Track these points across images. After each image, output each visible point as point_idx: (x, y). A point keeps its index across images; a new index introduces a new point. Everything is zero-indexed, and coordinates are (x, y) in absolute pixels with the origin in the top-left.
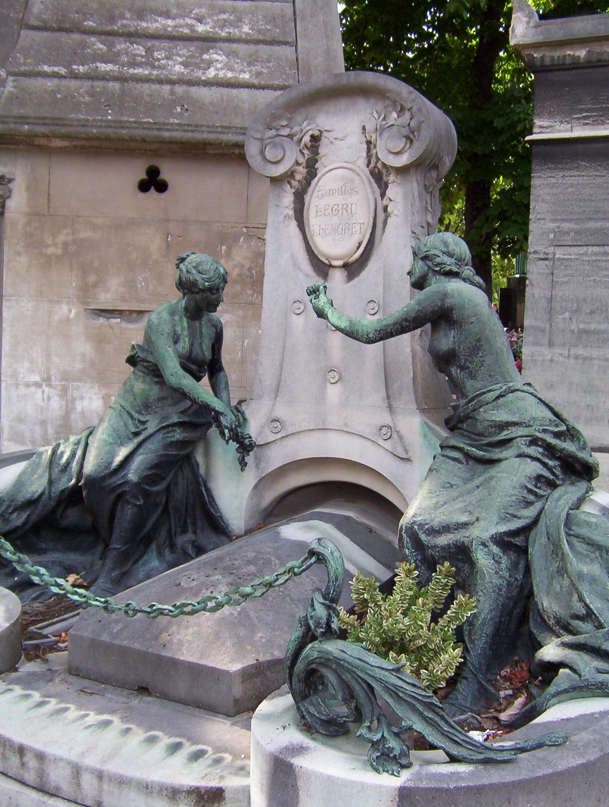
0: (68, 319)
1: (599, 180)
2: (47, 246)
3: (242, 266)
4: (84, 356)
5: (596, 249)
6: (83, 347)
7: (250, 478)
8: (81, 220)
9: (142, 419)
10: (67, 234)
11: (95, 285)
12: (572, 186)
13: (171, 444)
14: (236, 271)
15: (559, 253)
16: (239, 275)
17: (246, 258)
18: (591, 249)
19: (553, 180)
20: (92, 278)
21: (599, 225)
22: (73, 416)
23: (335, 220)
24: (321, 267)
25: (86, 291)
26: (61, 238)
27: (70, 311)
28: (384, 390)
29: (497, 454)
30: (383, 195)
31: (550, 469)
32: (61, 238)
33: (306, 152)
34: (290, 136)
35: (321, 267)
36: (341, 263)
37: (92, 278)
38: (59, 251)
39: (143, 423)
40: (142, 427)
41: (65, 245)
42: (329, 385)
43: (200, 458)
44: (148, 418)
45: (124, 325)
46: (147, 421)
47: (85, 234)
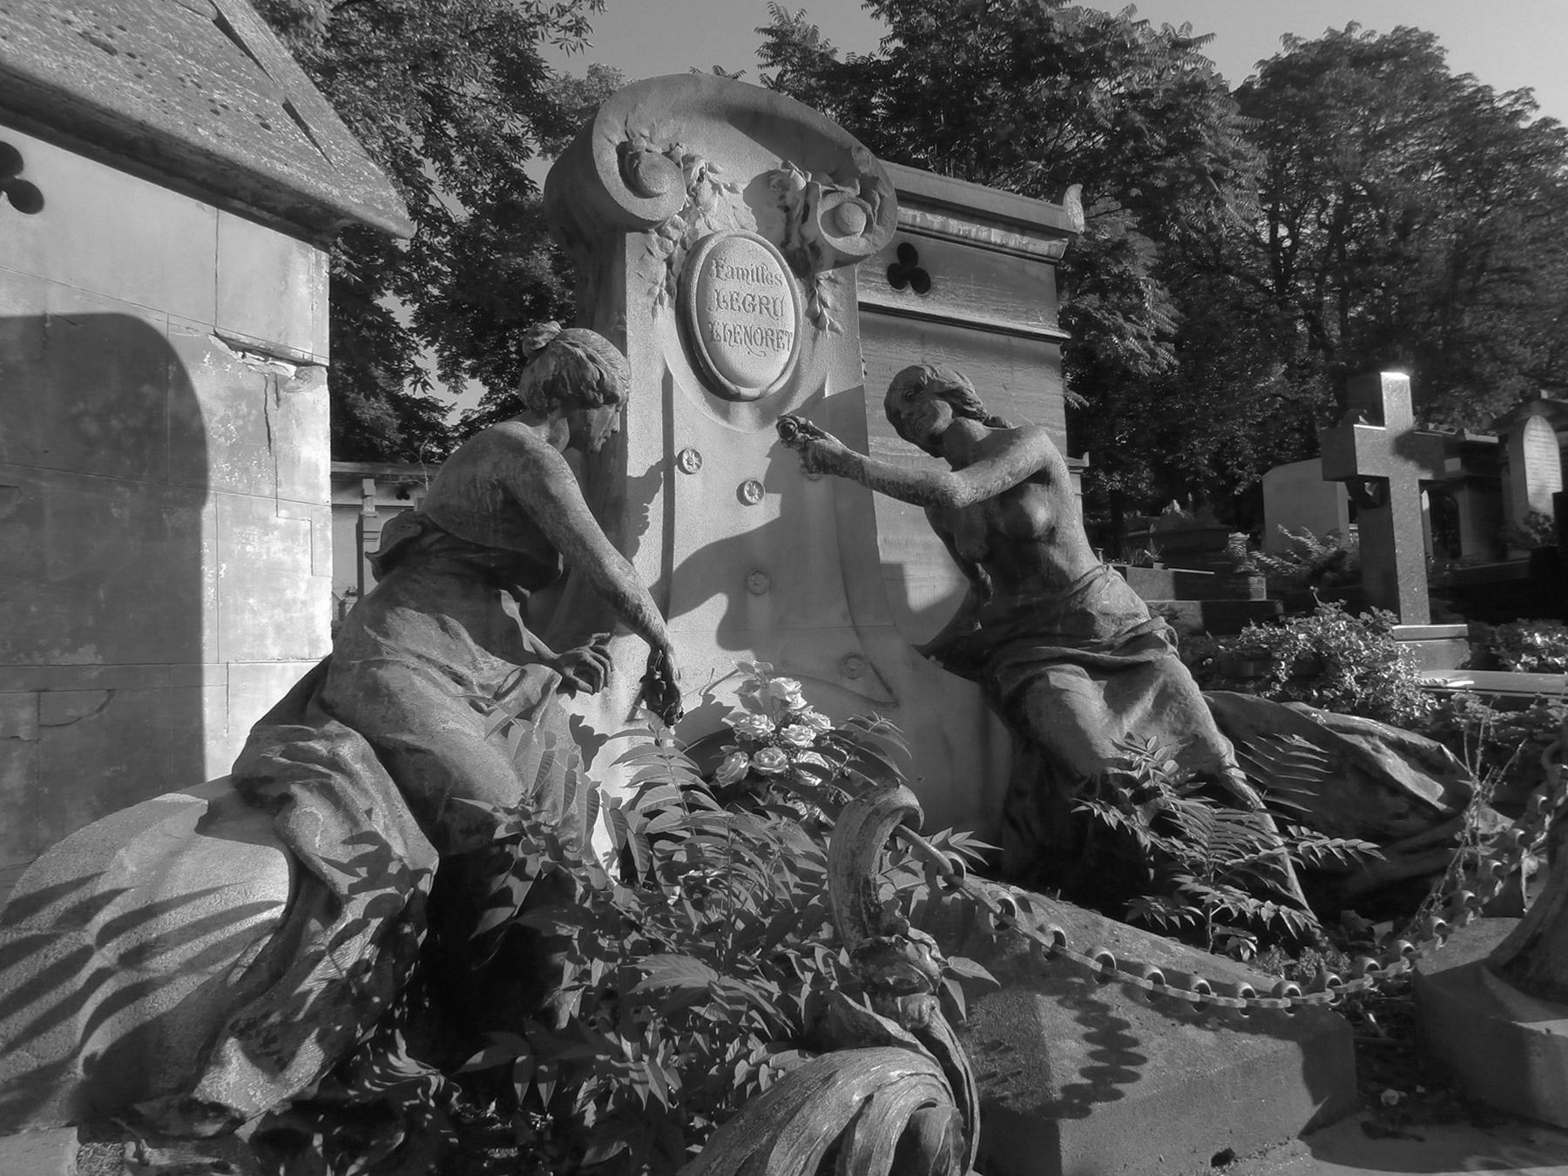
17: (218, 397)
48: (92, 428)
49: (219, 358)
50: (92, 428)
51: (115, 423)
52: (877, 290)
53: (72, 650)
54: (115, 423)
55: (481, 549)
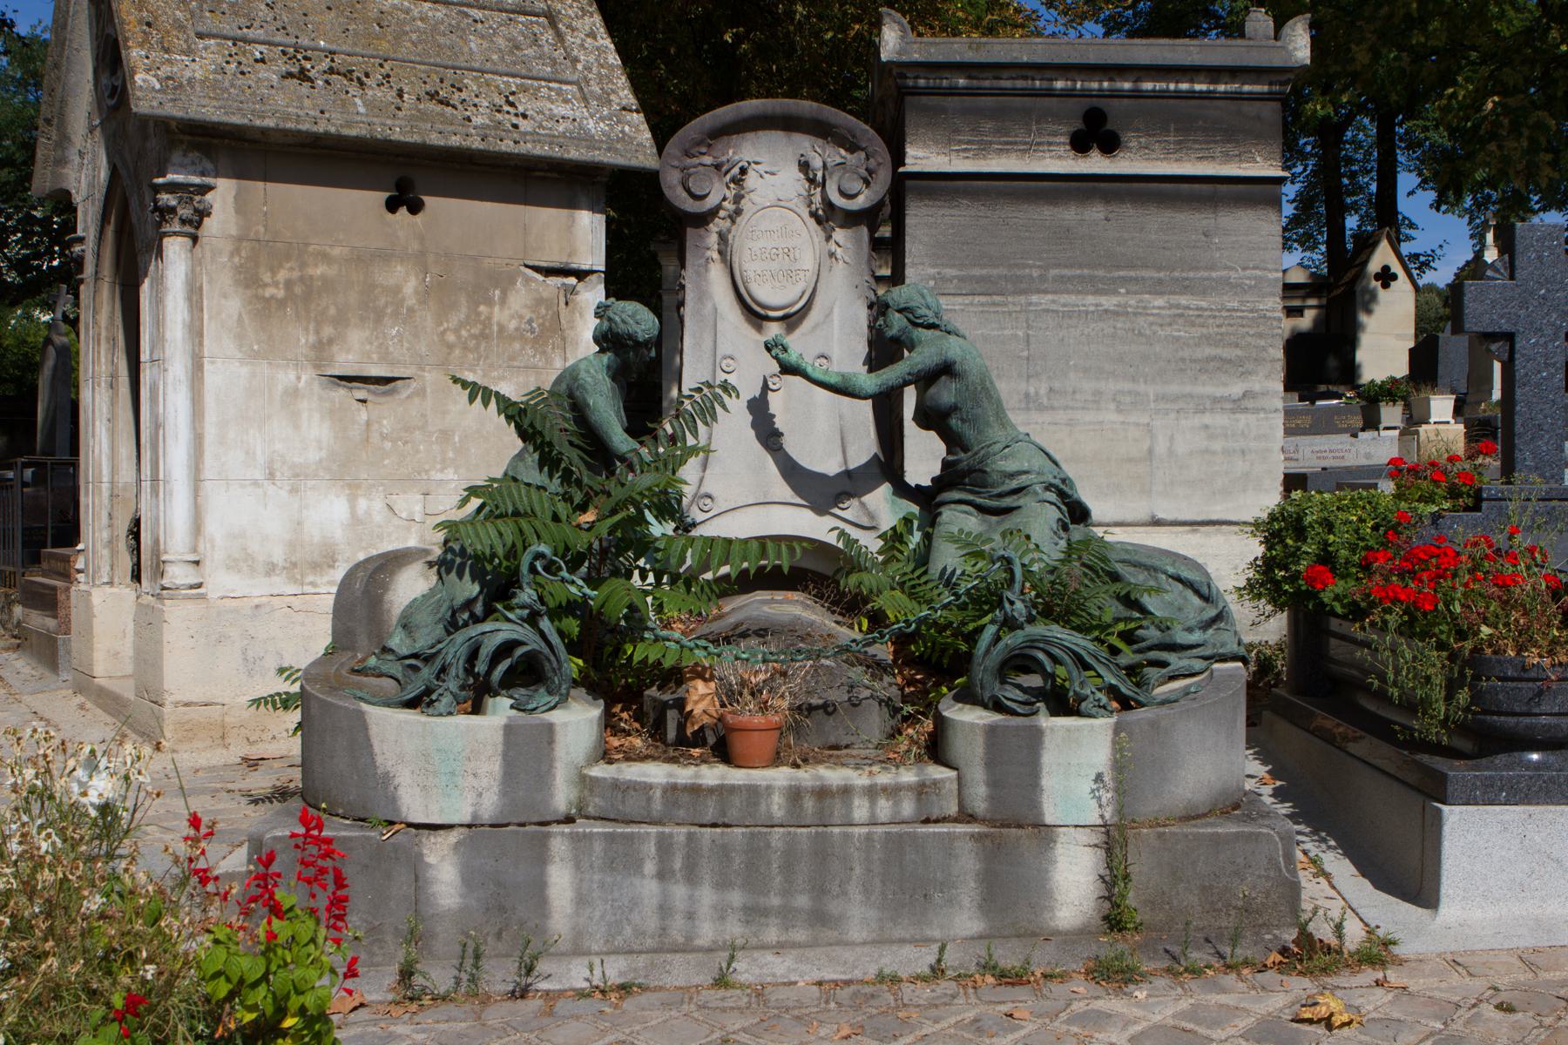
0: (296, 390)
2: (266, 285)
3: (521, 317)
4: (319, 441)
5: (983, 299)
8: (311, 249)
10: (292, 269)
11: (331, 341)
12: (953, 226)
14: (513, 325)
16: (517, 329)
17: (526, 306)
18: (977, 299)
19: (932, 220)
21: (984, 272)
23: (774, 266)
25: (321, 350)
26: (282, 275)
27: (299, 378)
29: (1008, 502)
30: (828, 238)
34: (718, 167)
35: (755, 315)
37: (328, 331)
38: (281, 294)
41: (289, 284)
47: (319, 270)
48: (451, 338)
49: (528, 280)
50: (451, 338)
51: (464, 333)
53: (442, 470)
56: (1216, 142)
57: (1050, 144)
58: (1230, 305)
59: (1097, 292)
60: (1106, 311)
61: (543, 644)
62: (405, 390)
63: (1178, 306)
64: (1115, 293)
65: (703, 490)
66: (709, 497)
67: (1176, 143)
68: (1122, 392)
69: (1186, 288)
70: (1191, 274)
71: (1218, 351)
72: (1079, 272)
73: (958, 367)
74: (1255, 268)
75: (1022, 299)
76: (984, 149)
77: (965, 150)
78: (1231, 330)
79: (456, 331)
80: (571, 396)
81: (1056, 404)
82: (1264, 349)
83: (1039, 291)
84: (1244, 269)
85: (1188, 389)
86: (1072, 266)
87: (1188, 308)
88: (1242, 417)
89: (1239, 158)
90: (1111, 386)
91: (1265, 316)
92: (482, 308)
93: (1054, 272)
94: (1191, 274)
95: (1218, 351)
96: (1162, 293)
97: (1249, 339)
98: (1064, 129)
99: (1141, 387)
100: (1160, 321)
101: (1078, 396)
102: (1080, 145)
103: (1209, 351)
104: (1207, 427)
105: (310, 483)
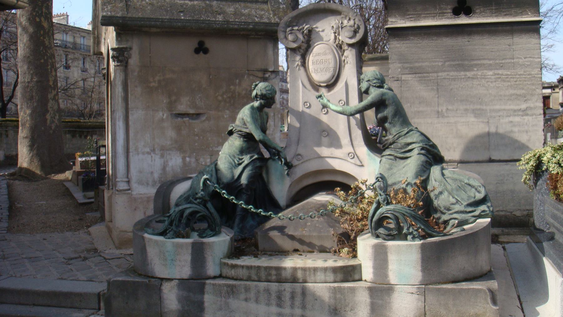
1: (419, 45)
6: (171, 133)
7: (288, 182)
9: (241, 157)
13: (257, 167)
14: (244, 92)
15: (404, 77)
16: (245, 94)
18: (417, 75)
19: (398, 45)
20: (174, 98)
22: (167, 169)
23: (322, 66)
24: (316, 87)
25: (171, 106)
26: (157, 78)
27: (163, 115)
28: (349, 137)
29: (408, 155)
31: (429, 159)
32: (157, 78)
33: (306, 37)
35: (316, 87)
36: (325, 84)
39: (242, 159)
40: (241, 162)
41: (159, 81)
42: (323, 138)
43: (264, 175)
44: (243, 157)
45: (191, 121)
46: (242, 159)
48: (220, 98)
50: (220, 98)
51: (225, 96)
52: (448, 18)
54: (225, 96)
55: (241, 131)
56: (512, 8)
57: (445, 13)
58: (519, 73)
59: (465, 70)
60: (469, 77)
61: (207, 212)
62: (203, 118)
63: (498, 74)
64: (473, 70)
65: (297, 153)
66: (299, 155)
67: (495, 9)
68: (477, 109)
69: (502, 67)
70: (503, 61)
71: (515, 92)
72: (457, 63)
73: (387, 102)
74: (531, 57)
75: (435, 75)
76: (418, 17)
77: (411, 18)
78: (520, 82)
79: (222, 96)
80: (243, 119)
81: (450, 115)
82: (535, 90)
83: (441, 72)
84: (525, 58)
85: (503, 107)
86: (455, 61)
87: (502, 75)
88: (526, 118)
89: (521, 14)
90: (471, 107)
91: (534, 77)
92: (232, 87)
93: (447, 63)
94: (503, 61)
95: (515, 92)
96: (491, 70)
97: (528, 86)
98: (449, 7)
99: (484, 107)
100: (491, 80)
101: (458, 112)
102: (456, 12)
103: (512, 92)
104: (511, 122)
105: (168, 152)
